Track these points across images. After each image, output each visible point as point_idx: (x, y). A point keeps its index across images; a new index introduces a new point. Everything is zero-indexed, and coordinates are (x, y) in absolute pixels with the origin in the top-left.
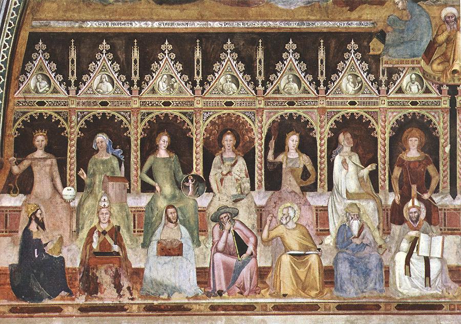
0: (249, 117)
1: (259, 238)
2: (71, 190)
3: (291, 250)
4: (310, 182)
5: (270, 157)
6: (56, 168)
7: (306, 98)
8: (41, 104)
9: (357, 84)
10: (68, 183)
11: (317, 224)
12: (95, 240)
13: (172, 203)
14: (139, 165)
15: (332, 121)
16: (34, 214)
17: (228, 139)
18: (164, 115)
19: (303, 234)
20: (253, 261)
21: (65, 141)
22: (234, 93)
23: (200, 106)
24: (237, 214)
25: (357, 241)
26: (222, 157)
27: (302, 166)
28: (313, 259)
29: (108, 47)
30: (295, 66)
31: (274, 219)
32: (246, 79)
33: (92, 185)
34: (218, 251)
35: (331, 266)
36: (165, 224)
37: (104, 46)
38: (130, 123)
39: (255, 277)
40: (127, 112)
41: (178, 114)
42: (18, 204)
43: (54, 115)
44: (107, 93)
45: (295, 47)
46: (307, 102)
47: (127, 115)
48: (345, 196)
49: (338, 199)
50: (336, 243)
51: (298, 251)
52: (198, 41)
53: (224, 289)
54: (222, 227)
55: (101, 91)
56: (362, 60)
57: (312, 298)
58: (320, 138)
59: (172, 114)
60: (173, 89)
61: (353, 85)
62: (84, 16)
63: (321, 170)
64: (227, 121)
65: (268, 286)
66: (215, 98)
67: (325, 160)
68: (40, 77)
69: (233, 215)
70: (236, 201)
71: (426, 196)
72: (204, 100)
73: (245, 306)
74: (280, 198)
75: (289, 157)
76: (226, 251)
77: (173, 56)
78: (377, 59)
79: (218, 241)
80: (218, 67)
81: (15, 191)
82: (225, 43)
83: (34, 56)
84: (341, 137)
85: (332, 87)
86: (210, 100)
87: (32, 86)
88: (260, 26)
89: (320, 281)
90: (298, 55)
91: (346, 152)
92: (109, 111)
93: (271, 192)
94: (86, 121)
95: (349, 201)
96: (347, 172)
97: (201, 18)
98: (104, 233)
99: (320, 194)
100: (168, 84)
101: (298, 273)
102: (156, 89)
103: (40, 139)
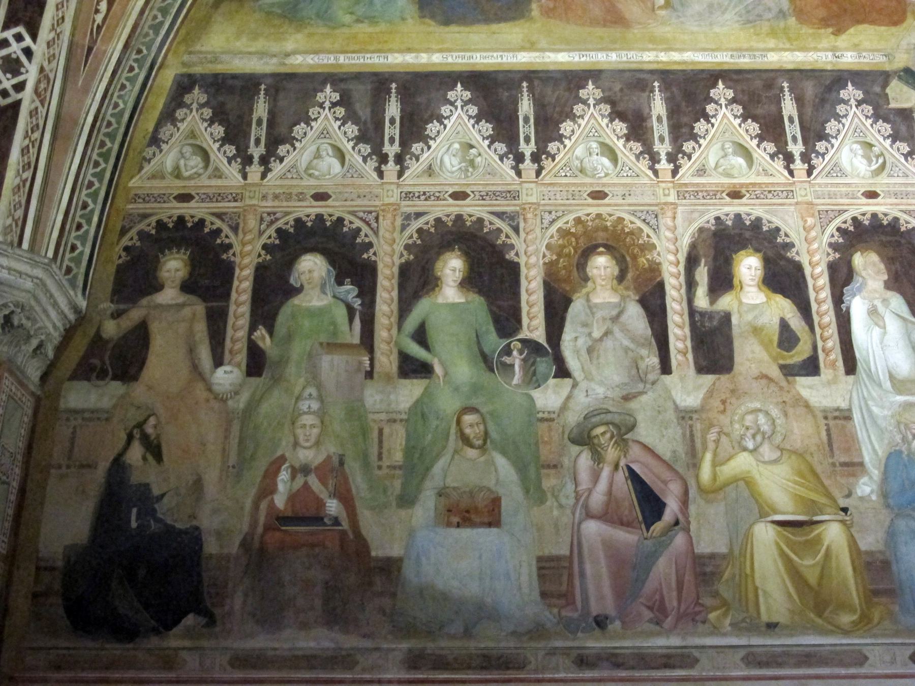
0: (644, 220)
1: (692, 483)
2: (231, 372)
3: (776, 512)
4: (801, 353)
5: (702, 301)
6: (201, 328)
7: (767, 184)
8: (185, 198)
9: (874, 159)
10: (227, 356)
11: (831, 450)
12: (281, 487)
13: (475, 402)
14: (394, 319)
15: (831, 228)
16: (140, 425)
18: (453, 217)
19: (800, 474)
20: (679, 540)
21: (226, 272)
22: (607, 175)
23: (533, 199)
24: (632, 427)
26: (588, 300)
27: (776, 321)
29: (336, 97)
30: (735, 128)
31: (724, 439)
32: (631, 149)
33: (283, 362)
34: (589, 515)
35: (880, 552)
36: (456, 452)
37: (328, 94)
38: (376, 233)
39: (688, 578)
40: (371, 212)
41: (486, 216)
42: (106, 403)
43: (209, 218)
44: (327, 177)
45: (730, 94)
46: (770, 192)
47: (371, 217)
48: (888, 385)
49: (874, 394)
50: (885, 495)
51: (793, 514)
52: (525, 84)
53: (610, 609)
54: (598, 457)
55: (317, 173)
56: (877, 116)
57: (846, 633)
58: (810, 264)
59: (470, 216)
60: (474, 167)
61: (865, 161)
62: (289, 46)
63: (822, 328)
64: (597, 229)
65: (725, 604)
66: (567, 185)
67: (828, 306)
68: (188, 150)
69: (623, 430)
70: (627, 398)
72: (543, 188)
73: (668, 656)
74: (733, 391)
75: (744, 300)
77: (473, 110)
79: (590, 491)
80: (569, 129)
81: (102, 375)
82: (583, 87)
83: (180, 113)
84: (858, 260)
86: (555, 189)
87: (169, 164)
88: (651, 58)
89: (857, 590)
90: (738, 109)
91: (875, 291)
92: (331, 209)
93: (709, 379)
94: (279, 231)
95: (900, 398)
96: (885, 333)
97: (531, 46)
98: (305, 470)
99: (829, 383)
100: (463, 160)
101: (802, 569)
102: (436, 169)
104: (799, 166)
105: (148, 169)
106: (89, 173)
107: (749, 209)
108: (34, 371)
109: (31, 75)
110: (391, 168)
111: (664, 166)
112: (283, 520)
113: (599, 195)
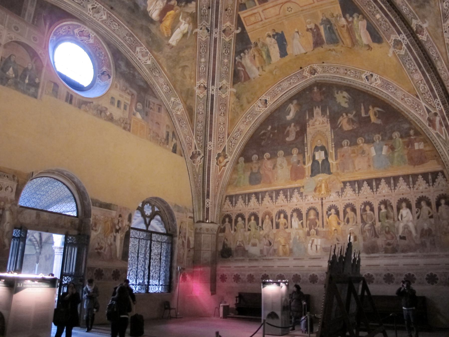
4: (286, 226)
5: (277, 221)
8: (227, 211)
15: (291, 210)
17: (267, 217)
20: (273, 247)
25: (298, 241)
28: (287, 246)
34: (265, 245)
48: (295, 229)
50: (293, 242)
56: (299, 194)
71: (316, 228)
76: (267, 245)
77: (255, 197)
78: (302, 193)
85: (291, 201)
90: (283, 194)
92: (241, 212)
93: (277, 230)
97: (261, 188)
98: (240, 241)
103: (227, 220)
104: (289, 202)
105: (224, 208)
106: (218, 213)
107: (283, 208)
108: (216, 233)
109: (210, 203)
110: (247, 206)
111: (274, 203)
112: (238, 246)
113: (267, 208)
